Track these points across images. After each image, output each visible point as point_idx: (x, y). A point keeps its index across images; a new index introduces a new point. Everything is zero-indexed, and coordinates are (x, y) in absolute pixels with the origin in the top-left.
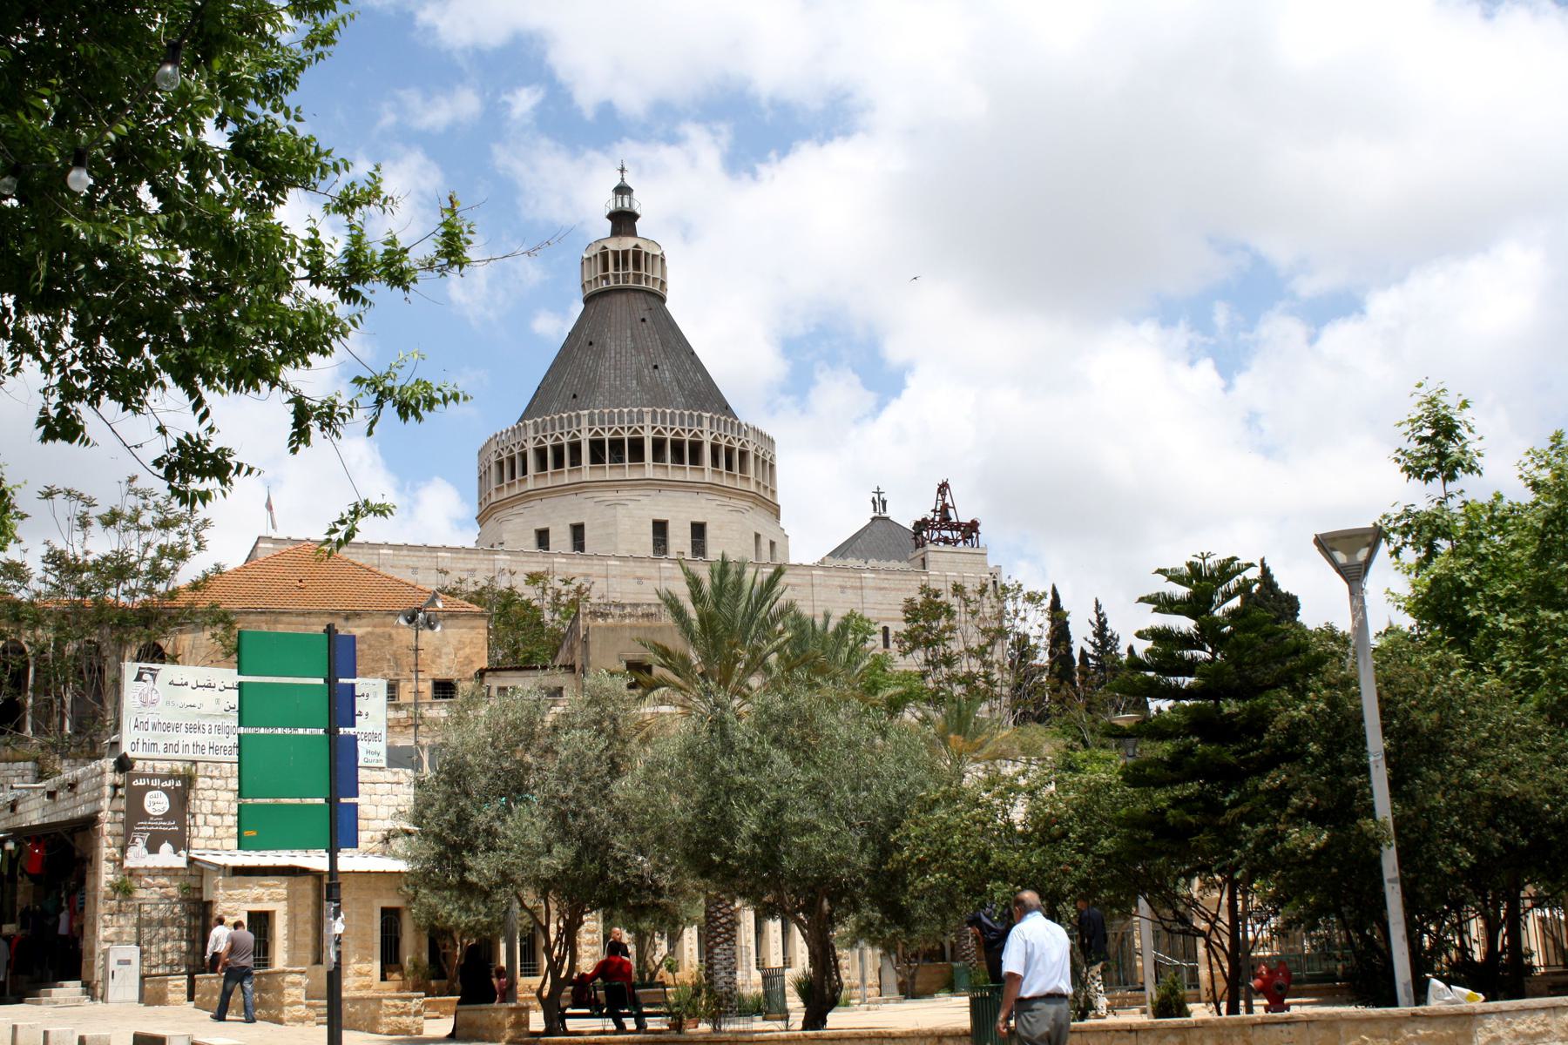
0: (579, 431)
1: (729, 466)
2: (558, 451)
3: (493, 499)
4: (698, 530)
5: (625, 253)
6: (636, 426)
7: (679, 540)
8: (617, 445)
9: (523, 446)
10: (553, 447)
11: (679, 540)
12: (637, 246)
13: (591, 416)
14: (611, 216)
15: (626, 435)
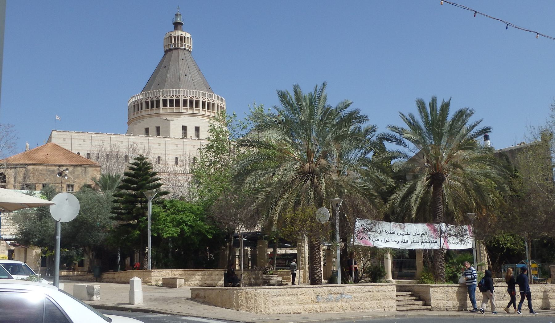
0: (159, 96)
1: (208, 108)
2: (152, 102)
3: (132, 117)
4: (197, 129)
5: (178, 36)
6: (178, 95)
7: (191, 132)
8: (171, 101)
9: (141, 101)
10: (151, 101)
11: (191, 132)
12: (182, 34)
13: (163, 91)
14: (173, 24)
15: (174, 98)
